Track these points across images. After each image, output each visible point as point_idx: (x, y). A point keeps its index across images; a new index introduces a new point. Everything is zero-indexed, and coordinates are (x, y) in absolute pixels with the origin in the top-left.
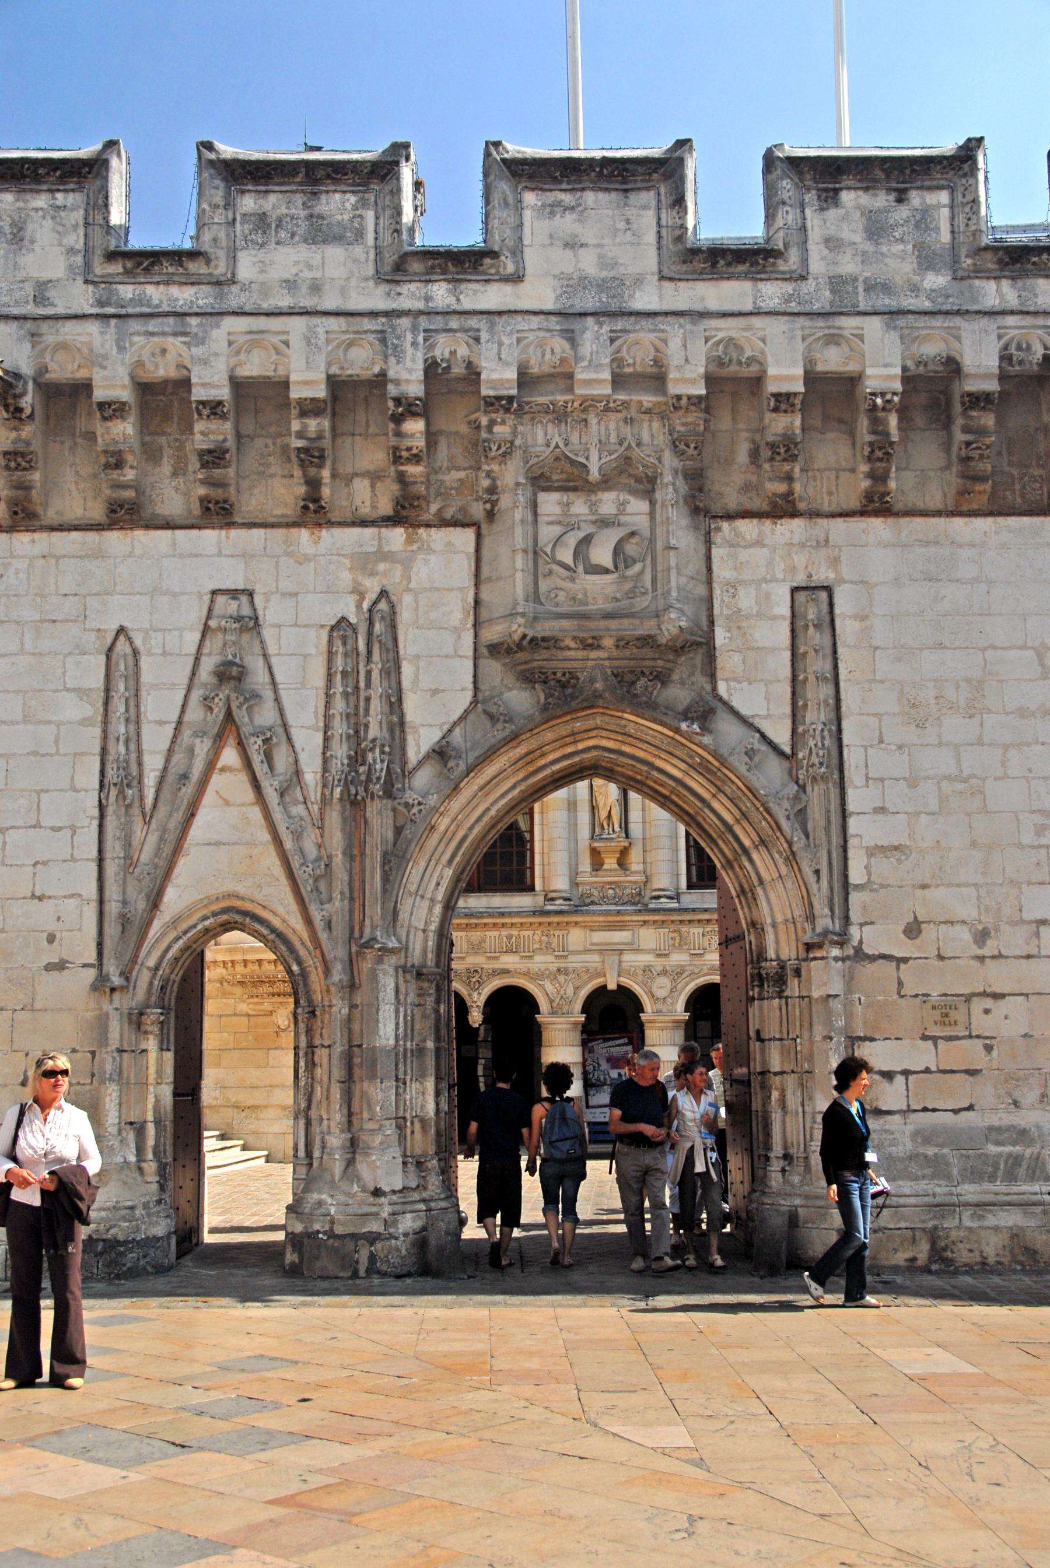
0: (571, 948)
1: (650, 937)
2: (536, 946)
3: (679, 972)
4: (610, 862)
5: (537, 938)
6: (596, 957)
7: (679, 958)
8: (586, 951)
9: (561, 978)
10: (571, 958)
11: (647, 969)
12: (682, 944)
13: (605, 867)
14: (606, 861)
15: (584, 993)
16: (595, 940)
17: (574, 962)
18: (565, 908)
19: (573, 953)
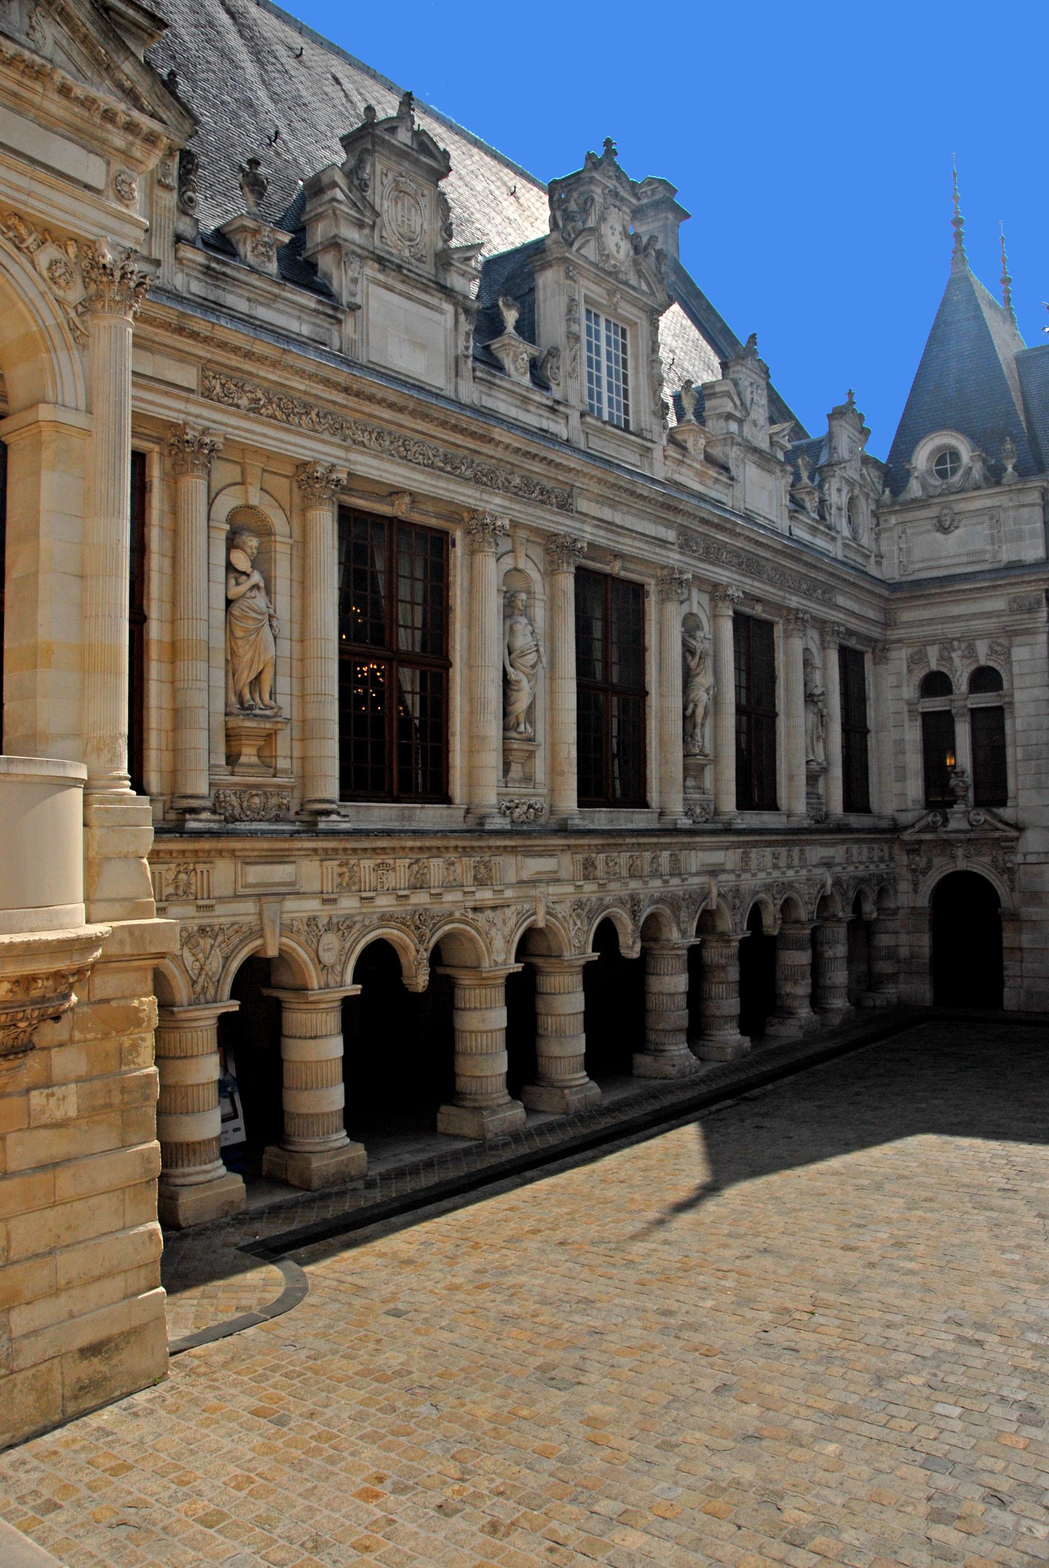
0: (216, 892)
1: (311, 872)
2: (171, 890)
3: (342, 926)
4: (248, 755)
5: (171, 875)
6: (250, 907)
7: (348, 904)
8: (237, 897)
9: (206, 943)
10: (220, 909)
11: (312, 921)
12: (349, 884)
13: (243, 759)
14: (246, 750)
15: (235, 965)
16: (251, 879)
17: (224, 914)
18: (215, 826)
19: (221, 899)
